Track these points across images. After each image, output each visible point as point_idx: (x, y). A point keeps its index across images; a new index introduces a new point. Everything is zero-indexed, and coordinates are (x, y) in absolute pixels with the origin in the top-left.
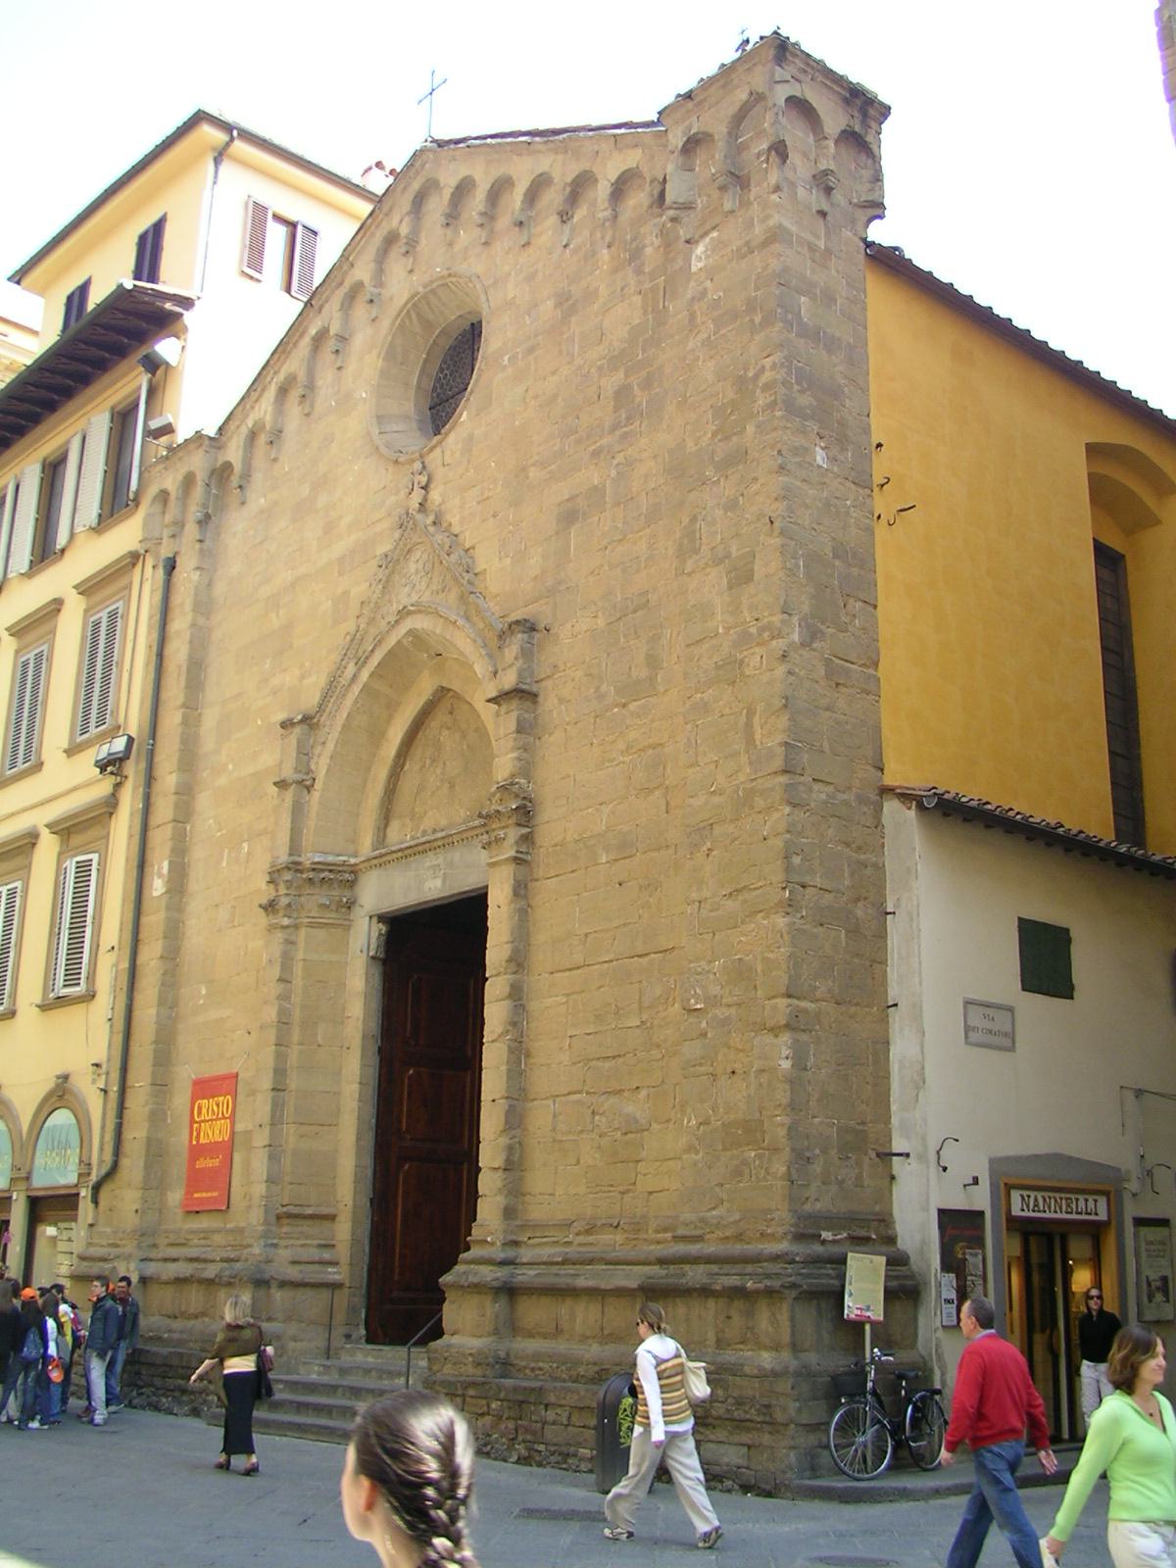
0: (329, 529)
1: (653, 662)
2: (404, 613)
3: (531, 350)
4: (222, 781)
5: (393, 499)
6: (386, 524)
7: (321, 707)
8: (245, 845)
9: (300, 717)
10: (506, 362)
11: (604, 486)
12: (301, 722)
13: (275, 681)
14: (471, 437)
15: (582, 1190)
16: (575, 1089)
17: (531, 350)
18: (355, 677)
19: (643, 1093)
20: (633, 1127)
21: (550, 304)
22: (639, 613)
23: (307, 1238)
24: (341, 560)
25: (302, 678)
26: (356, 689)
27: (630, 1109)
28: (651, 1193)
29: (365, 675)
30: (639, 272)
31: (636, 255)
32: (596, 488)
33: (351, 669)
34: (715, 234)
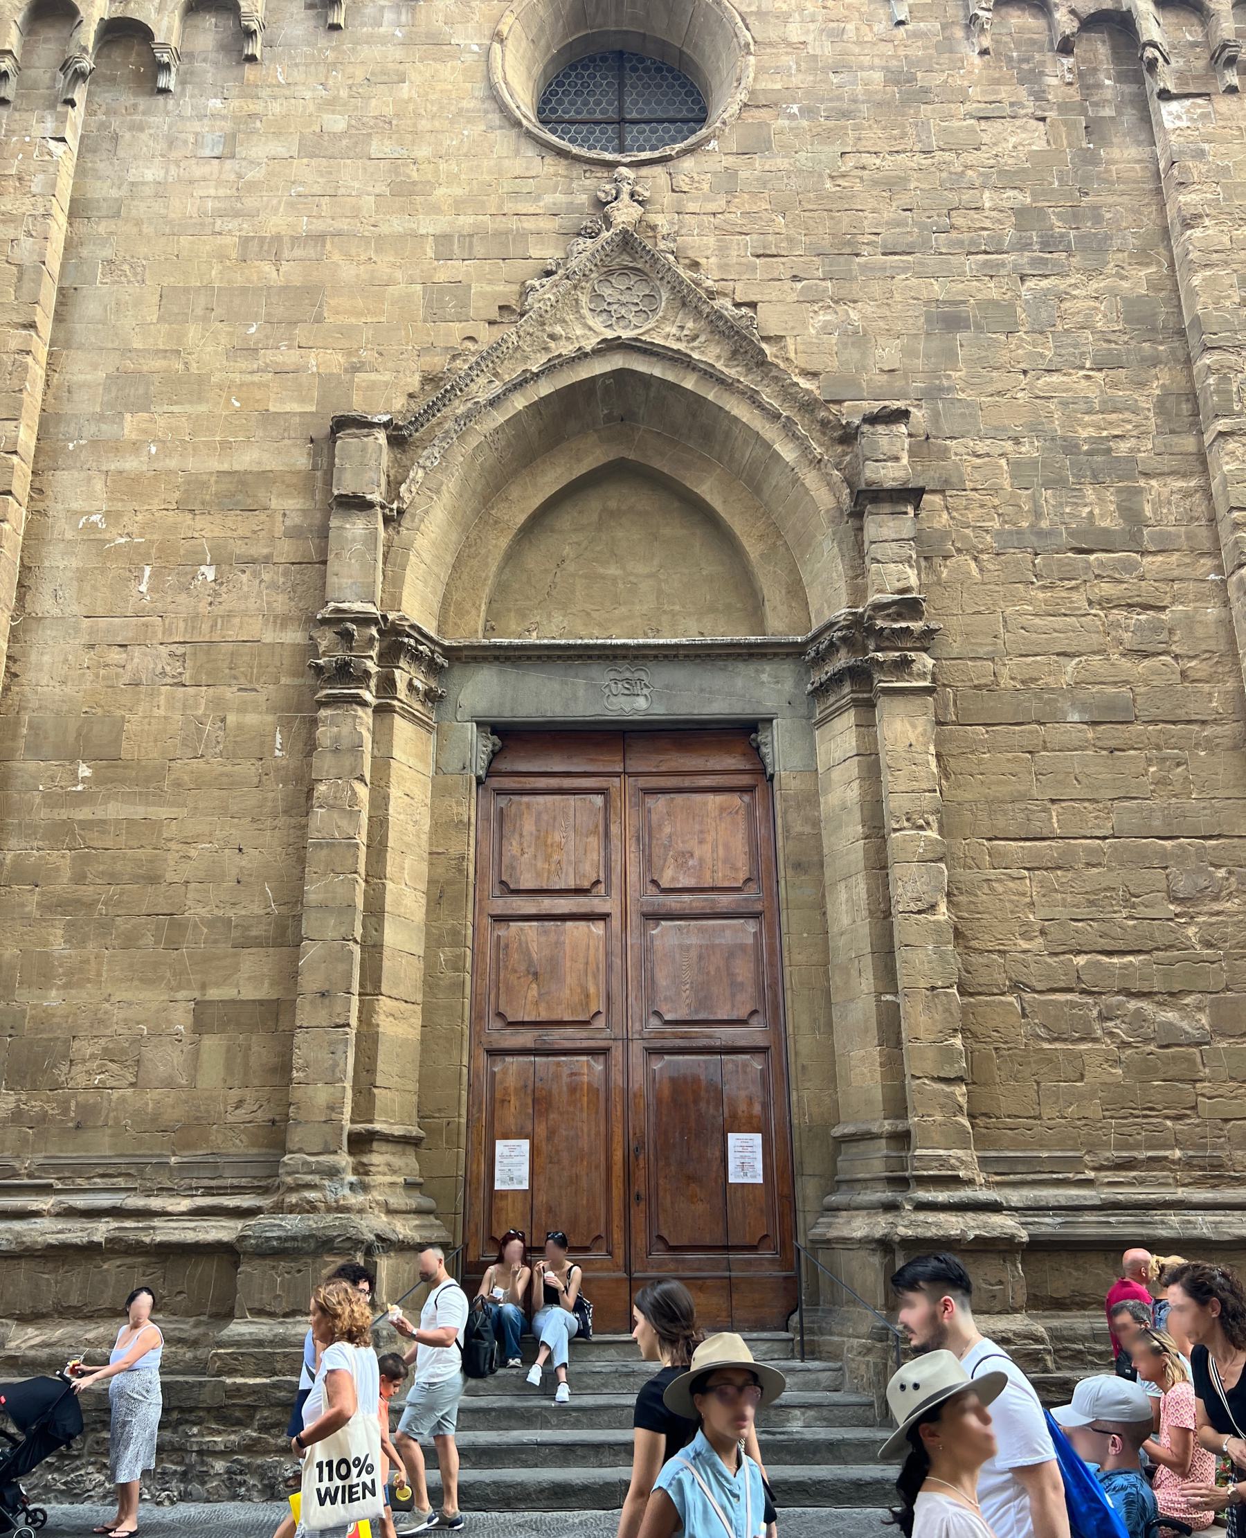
0: (405, 192)
1: (1131, 515)
2: (611, 346)
3: (846, 115)
4: (131, 464)
5: (560, 198)
6: (554, 224)
7: (417, 422)
8: (210, 573)
9: (385, 418)
10: (795, 109)
11: (1011, 306)
12: (386, 425)
13: (287, 357)
14: (731, 173)
15: (1094, 1109)
16: (1062, 985)
17: (846, 115)
18: (493, 403)
19: (1188, 1000)
20: (1170, 1039)
21: (878, 76)
22: (1099, 458)
23: (394, 1172)
24: (443, 240)
25: (355, 369)
26: (499, 417)
27: (1170, 1016)
28: (1226, 1120)
29: (519, 402)
30: (1039, 96)
31: (1032, 78)
32: (994, 303)
33: (483, 389)
34: (1199, 101)
